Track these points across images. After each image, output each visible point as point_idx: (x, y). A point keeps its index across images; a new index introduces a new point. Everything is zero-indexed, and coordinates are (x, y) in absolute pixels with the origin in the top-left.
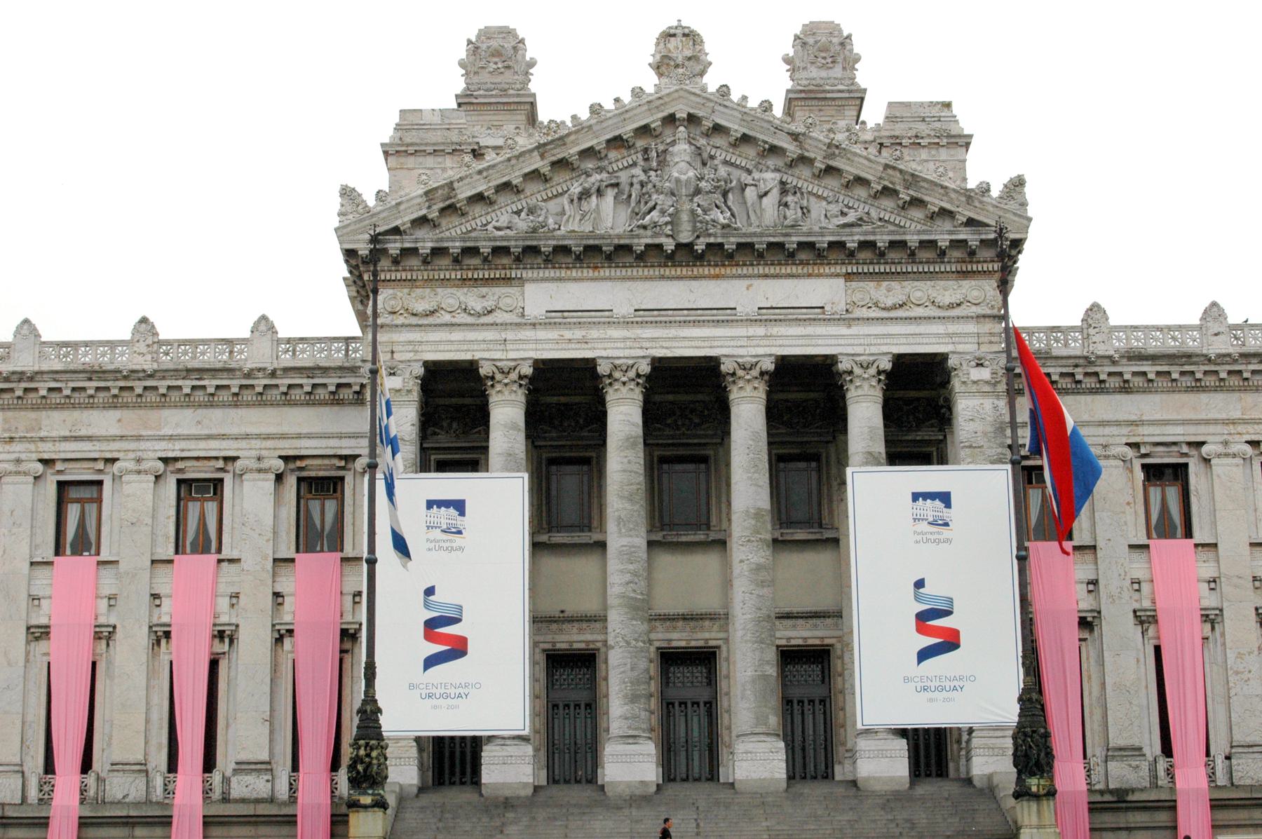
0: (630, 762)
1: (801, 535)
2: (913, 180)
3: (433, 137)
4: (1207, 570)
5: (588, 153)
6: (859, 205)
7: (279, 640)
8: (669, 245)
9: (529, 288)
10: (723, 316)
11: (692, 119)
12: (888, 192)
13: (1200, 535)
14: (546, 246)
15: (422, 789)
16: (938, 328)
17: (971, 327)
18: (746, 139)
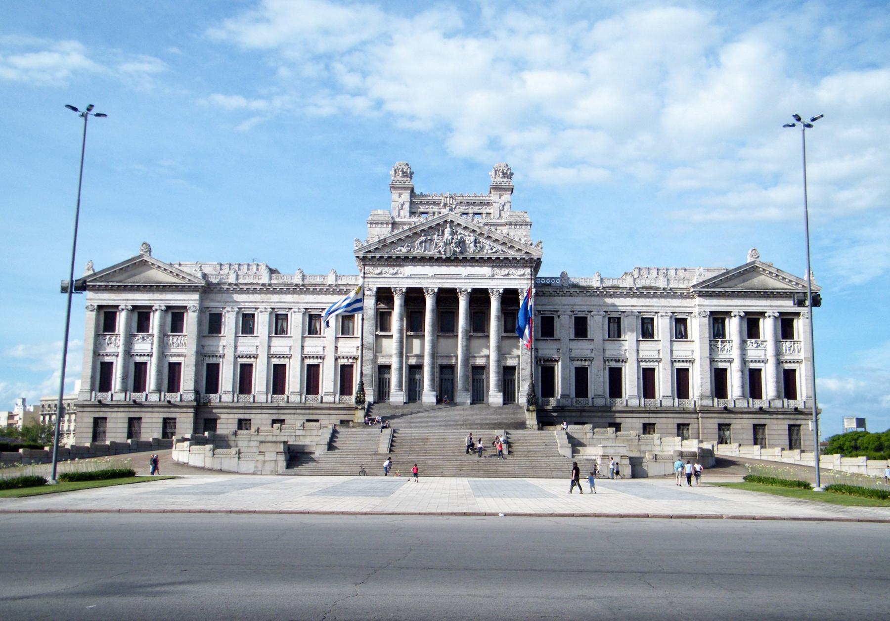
0: (428, 396)
1: (479, 334)
2: (511, 241)
3: (381, 218)
4: (591, 347)
5: (423, 230)
6: (497, 247)
7: (336, 359)
8: (444, 257)
9: (405, 268)
10: (458, 277)
11: (452, 221)
12: (504, 244)
13: (589, 337)
14: (411, 257)
15: (375, 402)
16: (517, 281)
17: (526, 281)
18: (466, 228)
